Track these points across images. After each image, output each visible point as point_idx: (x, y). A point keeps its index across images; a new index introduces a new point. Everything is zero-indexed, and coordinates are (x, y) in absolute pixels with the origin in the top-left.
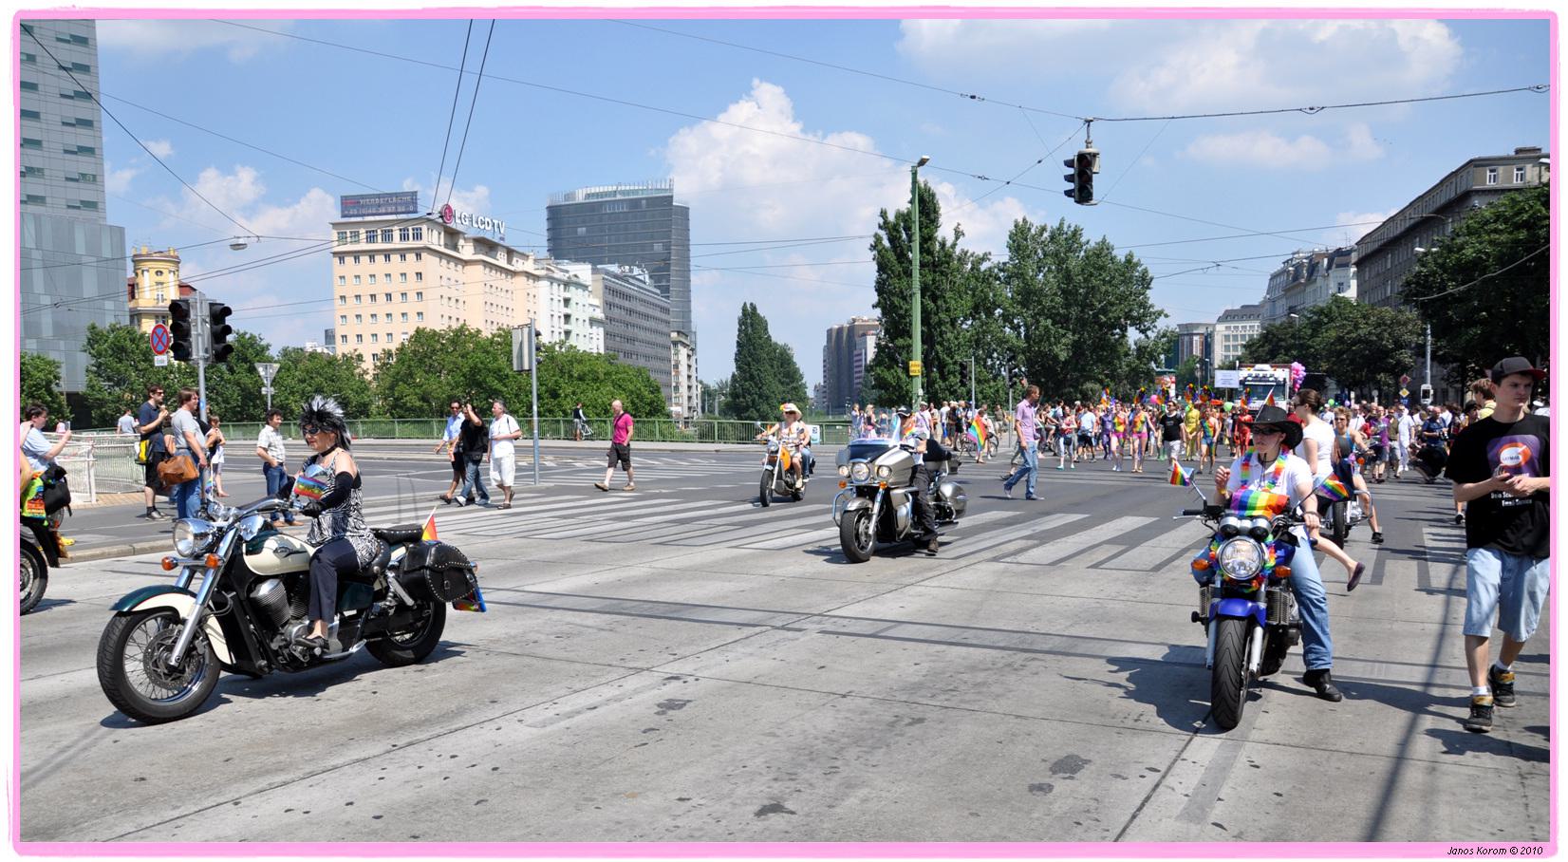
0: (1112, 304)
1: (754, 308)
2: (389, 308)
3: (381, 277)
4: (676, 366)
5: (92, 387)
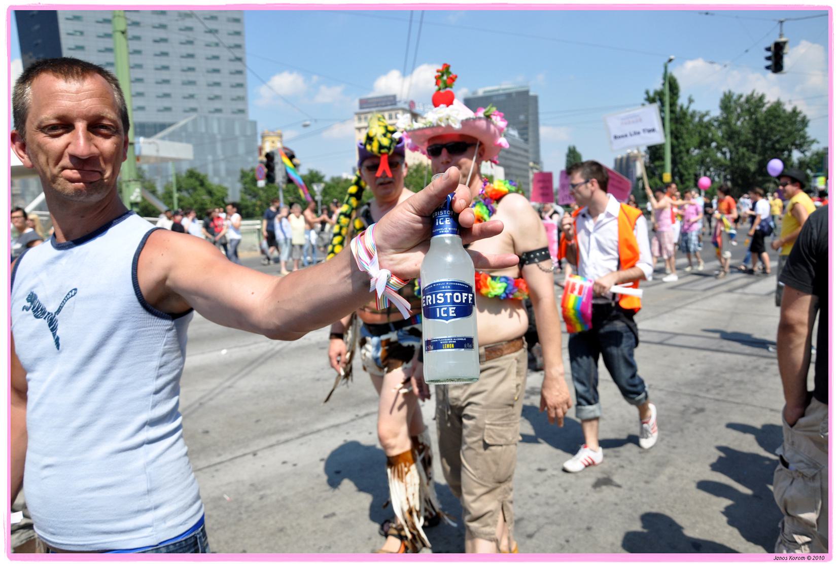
0: (783, 137)
1: (574, 148)
5: (242, 199)
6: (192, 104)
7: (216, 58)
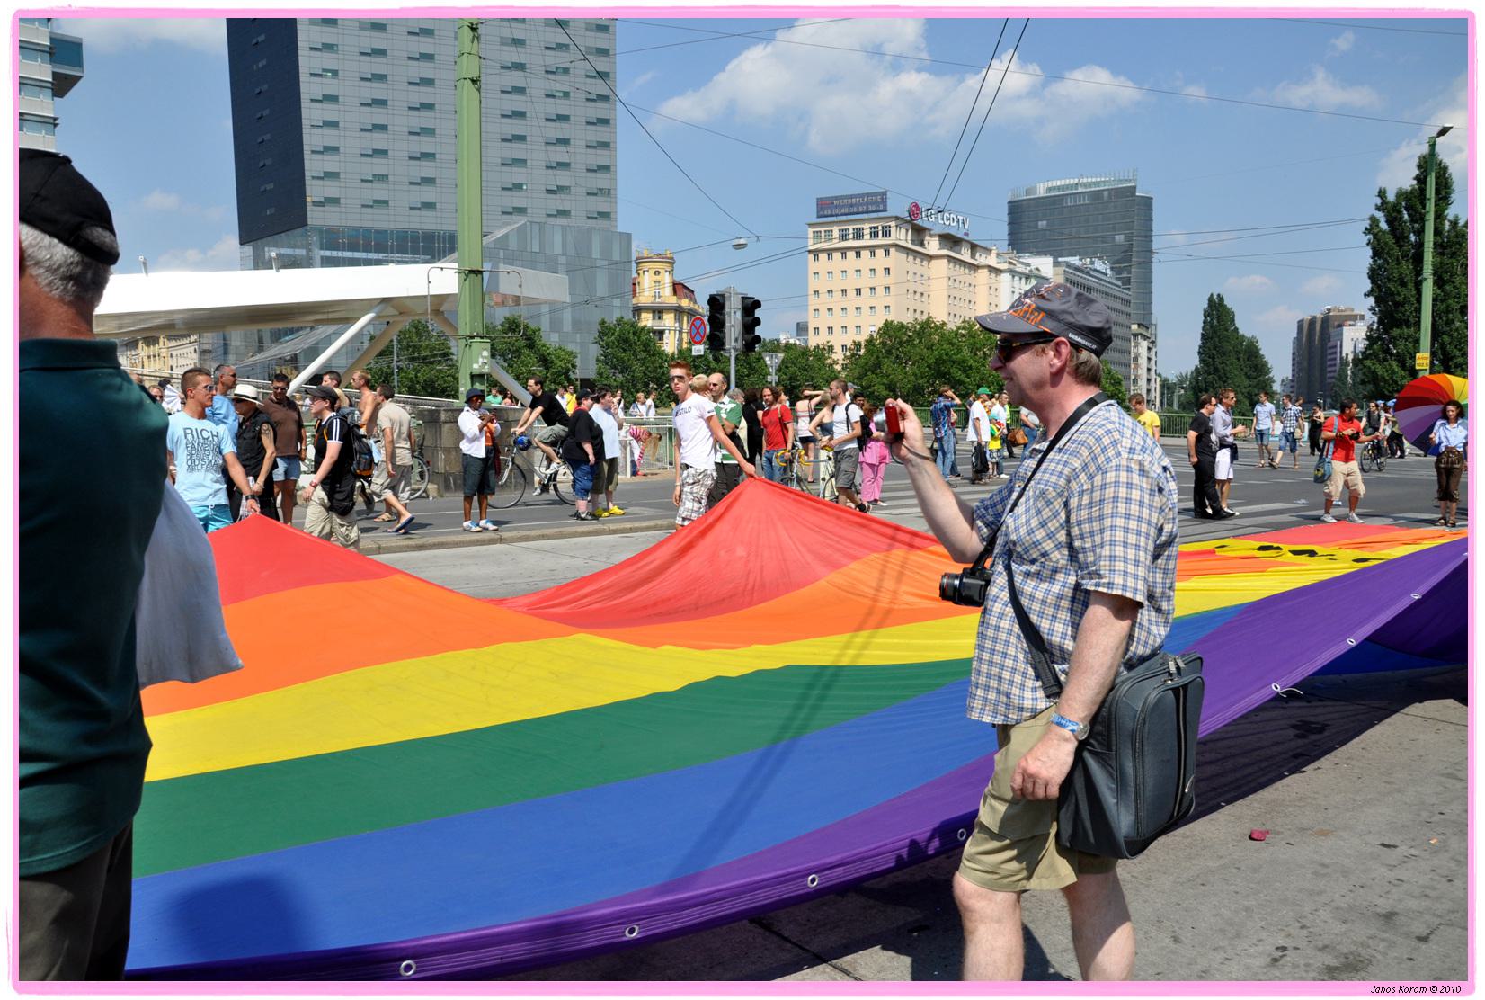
1: (1221, 298)
2: (858, 302)
3: (851, 272)
4: (1136, 359)
5: (601, 375)
6: (517, 200)
7: (563, 118)
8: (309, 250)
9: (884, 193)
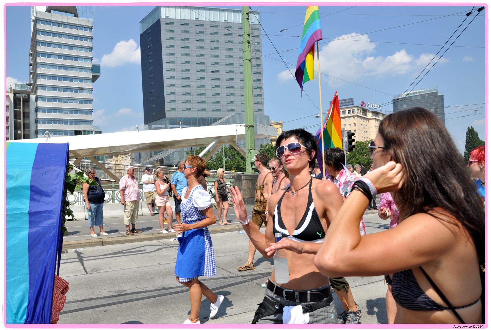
6: (232, 106)
8: (166, 125)
9: (352, 99)
